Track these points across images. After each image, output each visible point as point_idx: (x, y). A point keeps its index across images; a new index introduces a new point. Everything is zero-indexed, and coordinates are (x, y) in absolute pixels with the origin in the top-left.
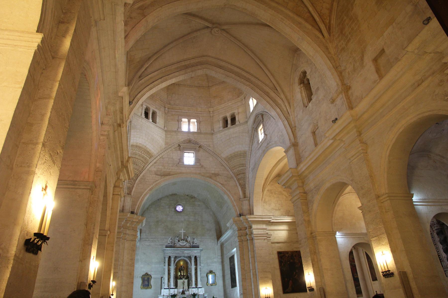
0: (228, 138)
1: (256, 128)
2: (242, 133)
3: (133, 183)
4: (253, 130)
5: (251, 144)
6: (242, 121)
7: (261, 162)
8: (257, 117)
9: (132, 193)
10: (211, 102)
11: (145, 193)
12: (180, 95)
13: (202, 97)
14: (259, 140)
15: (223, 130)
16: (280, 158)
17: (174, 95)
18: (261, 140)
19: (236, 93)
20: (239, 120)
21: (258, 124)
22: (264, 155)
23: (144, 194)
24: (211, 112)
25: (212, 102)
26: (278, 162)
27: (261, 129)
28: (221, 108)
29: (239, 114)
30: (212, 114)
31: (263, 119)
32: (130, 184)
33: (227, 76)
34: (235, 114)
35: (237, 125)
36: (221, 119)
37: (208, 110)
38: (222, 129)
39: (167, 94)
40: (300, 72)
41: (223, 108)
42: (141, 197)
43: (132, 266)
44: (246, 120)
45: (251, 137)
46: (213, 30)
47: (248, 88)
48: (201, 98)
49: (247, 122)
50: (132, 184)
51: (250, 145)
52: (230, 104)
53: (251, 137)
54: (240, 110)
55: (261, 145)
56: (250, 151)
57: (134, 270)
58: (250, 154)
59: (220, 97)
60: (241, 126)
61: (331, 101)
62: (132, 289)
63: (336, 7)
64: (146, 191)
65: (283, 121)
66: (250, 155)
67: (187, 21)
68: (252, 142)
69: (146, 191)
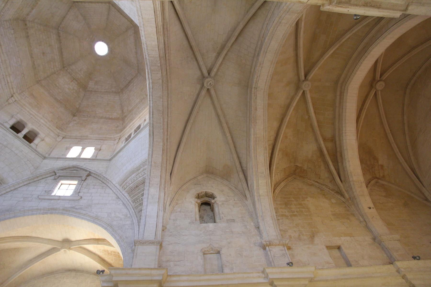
0: (5, 143)
1: (59, 176)
2: (28, 160)
4: (50, 173)
5: (25, 183)
6: (40, 150)
7: (26, 217)
8: (73, 169)
10: (22, 92)
12: (16, 42)
13: (24, 76)
14: (53, 191)
15: (8, 129)
16: (34, 235)
17: (12, 31)
18: (53, 194)
19: (57, 123)
20: (37, 146)
21: (71, 176)
22: (46, 213)
24: (12, 98)
25: (24, 93)
26: (24, 237)
27: (62, 183)
28: (28, 112)
29: (43, 140)
30: (12, 102)
31: (86, 179)
33: (163, 112)
34: (39, 135)
35: (30, 146)
36: (18, 119)
37: (14, 93)
38: (9, 126)
39: (10, 20)
40: (204, 191)
41: (31, 114)
44: (47, 155)
45: (37, 177)
46: (212, 80)
47: (162, 144)
48: (23, 75)
49: (45, 158)
51: (23, 182)
52: (42, 121)
53: (37, 177)
54: (47, 139)
55: (55, 200)
56: (12, 188)
58: (8, 190)
59: (38, 103)
60: (34, 153)
61: (267, 243)
63: (282, 187)
65: (159, 209)
66: (5, 192)
67: (217, 47)
68: (30, 183)
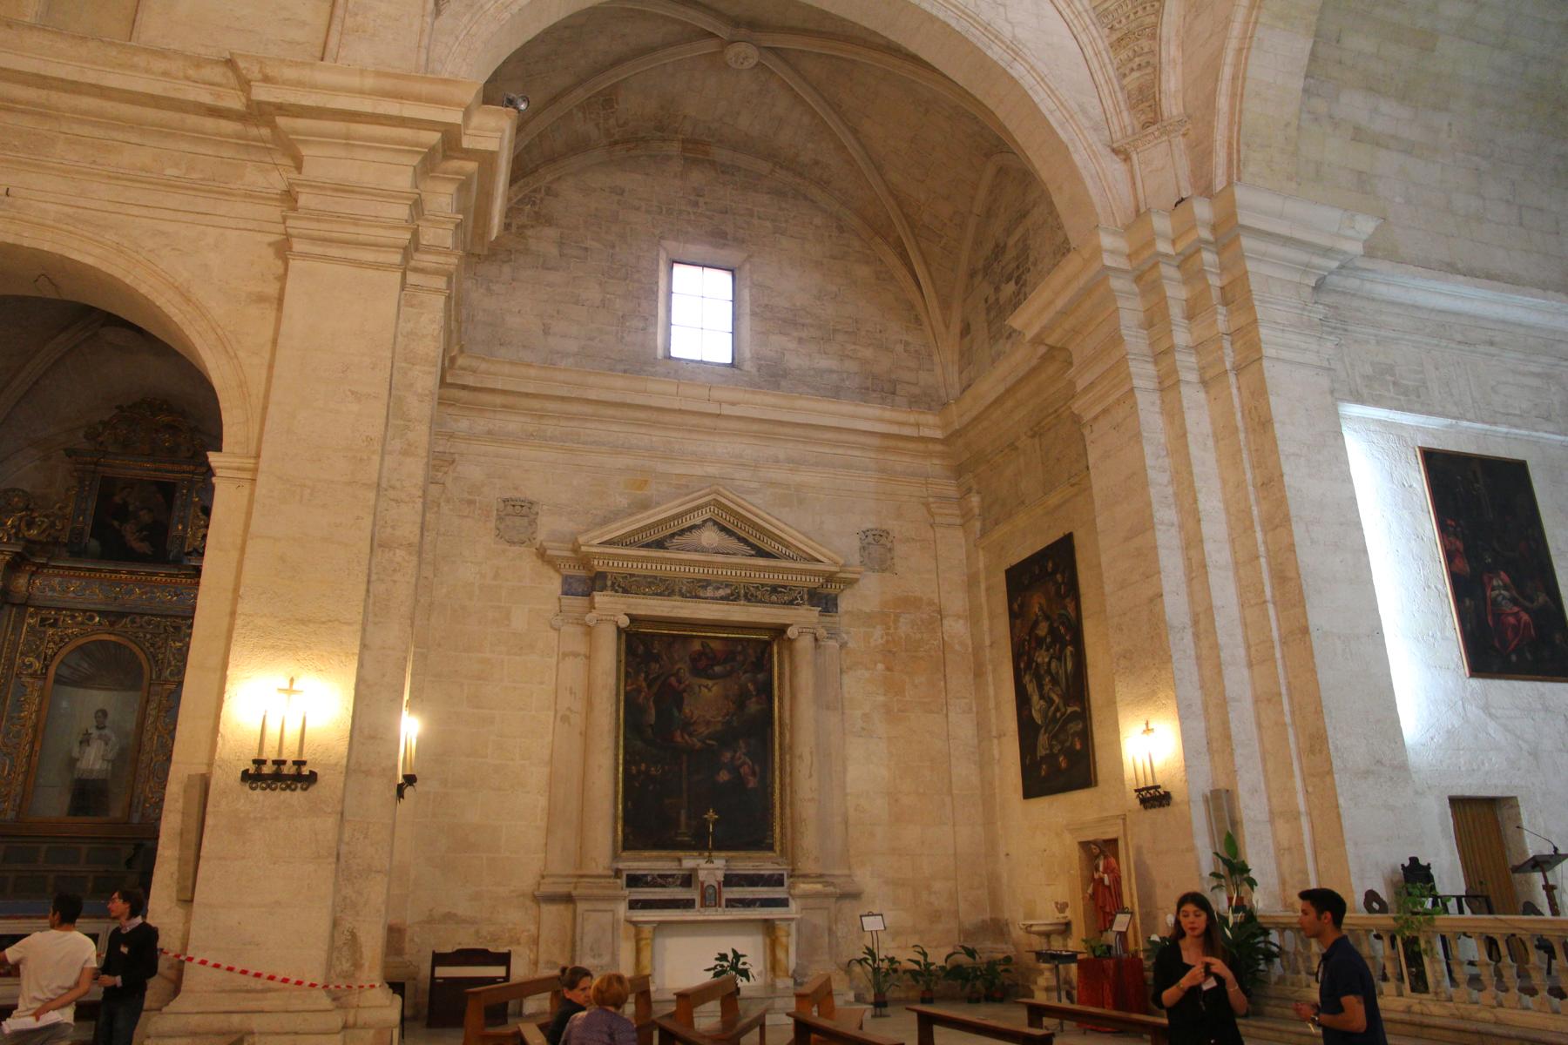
3: (1152, 52)
9: (1172, 107)
11: (1233, 44)
23: (1229, 57)
32: (1136, 74)
42: (1224, 87)
43: (1277, 527)
50: (1148, 63)
57: (1291, 548)
62: (1313, 671)
64: (1236, 29)
69: (1236, 29)
